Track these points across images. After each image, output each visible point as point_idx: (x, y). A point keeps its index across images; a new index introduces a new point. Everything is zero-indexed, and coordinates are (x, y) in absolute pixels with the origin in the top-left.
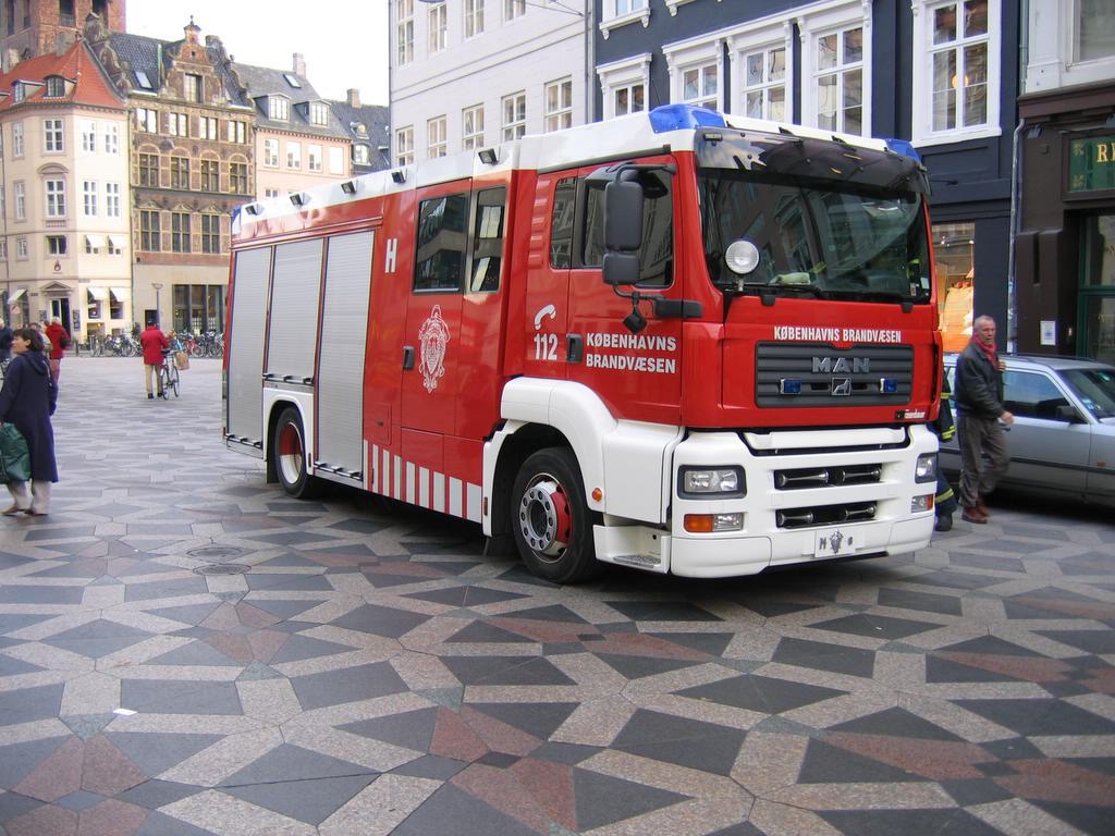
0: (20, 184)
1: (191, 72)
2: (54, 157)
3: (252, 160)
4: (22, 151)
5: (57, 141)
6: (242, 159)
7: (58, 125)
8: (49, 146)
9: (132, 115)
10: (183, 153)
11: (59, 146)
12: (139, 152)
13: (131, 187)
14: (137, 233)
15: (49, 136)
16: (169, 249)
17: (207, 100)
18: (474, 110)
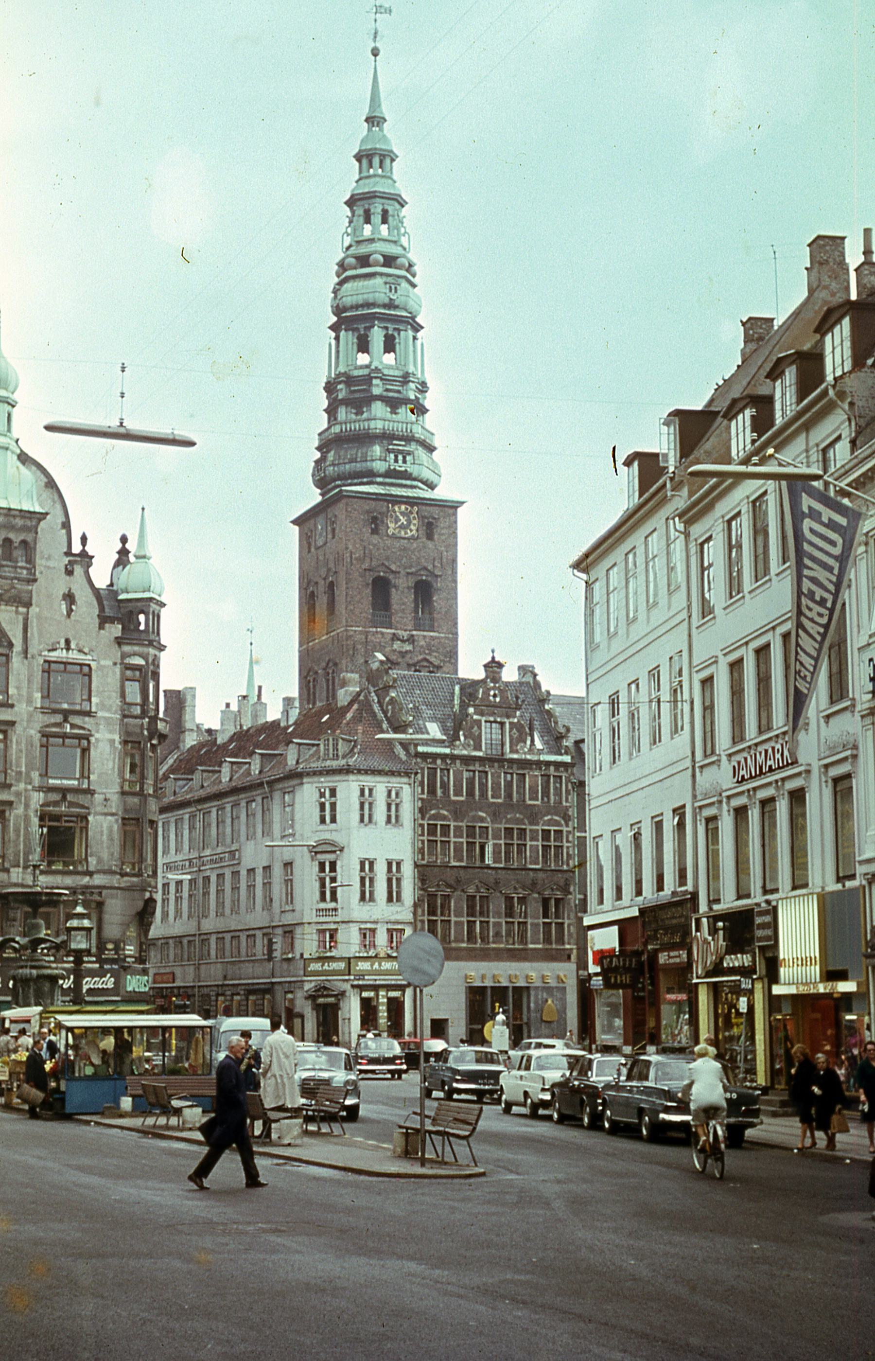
0: (288, 865)
1: (492, 719)
2: (327, 833)
3: (570, 823)
4: (292, 826)
5: (328, 813)
6: (558, 824)
7: (333, 793)
8: (323, 821)
9: (419, 776)
10: (482, 820)
11: (333, 820)
12: (425, 823)
13: (416, 865)
14: (423, 921)
15: (322, 806)
16: (463, 941)
17: (511, 751)
18: (228, 937)
